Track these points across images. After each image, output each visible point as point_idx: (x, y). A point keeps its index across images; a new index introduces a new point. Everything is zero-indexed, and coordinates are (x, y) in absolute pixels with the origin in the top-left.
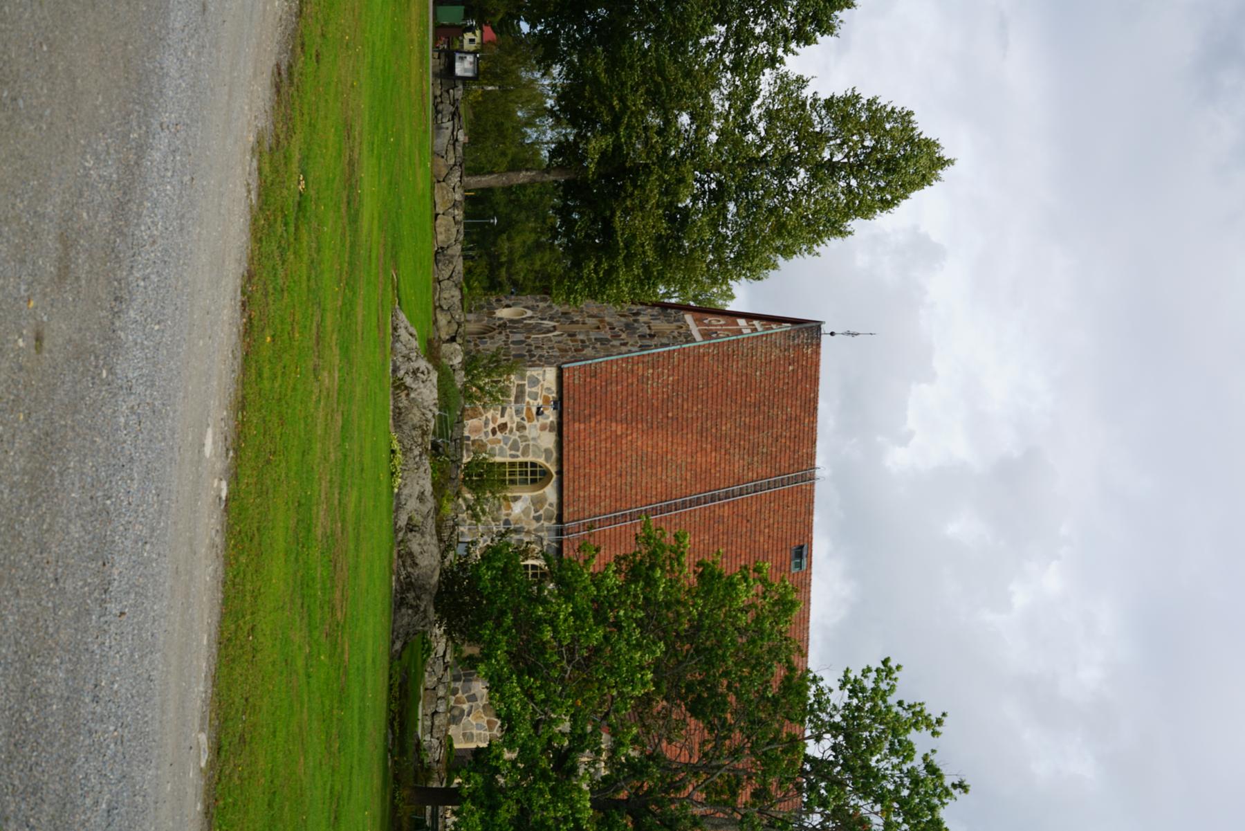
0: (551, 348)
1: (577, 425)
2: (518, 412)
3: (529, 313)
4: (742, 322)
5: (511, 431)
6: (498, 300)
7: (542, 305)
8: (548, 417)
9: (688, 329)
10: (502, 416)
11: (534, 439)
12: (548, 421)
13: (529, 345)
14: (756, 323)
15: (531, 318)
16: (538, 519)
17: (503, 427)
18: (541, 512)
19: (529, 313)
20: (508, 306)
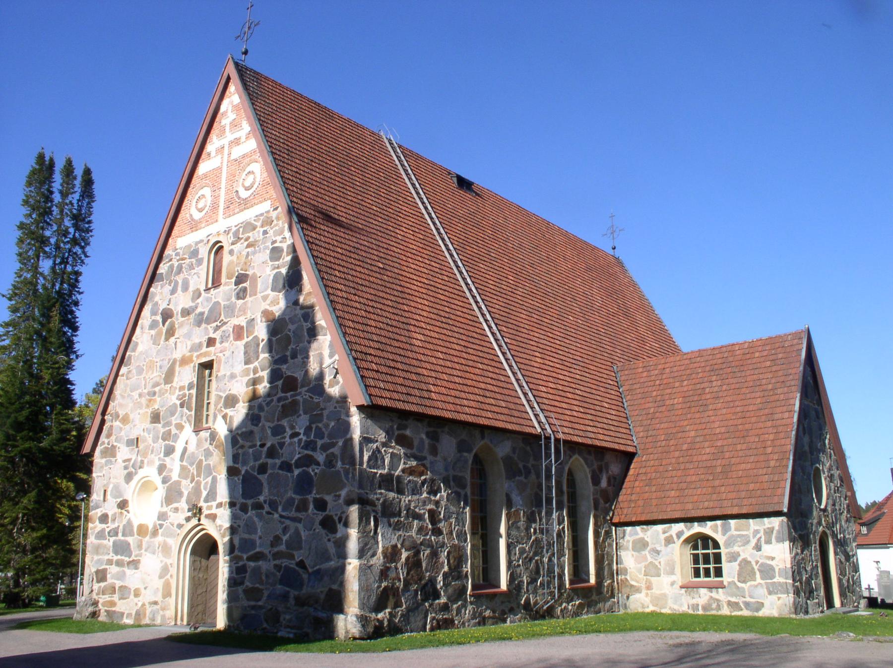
0: (278, 431)
1: (433, 395)
2: (415, 491)
3: (150, 472)
4: (203, 168)
5: (437, 503)
6: (104, 518)
7: (124, 452)
8: (422, 440)
9: (227, 232)
10: (419, 517)
11: (446, 469)
12: (427, 441)
13: (263, 469)
14: (210, 148)
15: (162, 468)
16: (528, 473)
17: (433, 515)
18: (521, 466)
19: (150, 472)
20: (123, 505)
